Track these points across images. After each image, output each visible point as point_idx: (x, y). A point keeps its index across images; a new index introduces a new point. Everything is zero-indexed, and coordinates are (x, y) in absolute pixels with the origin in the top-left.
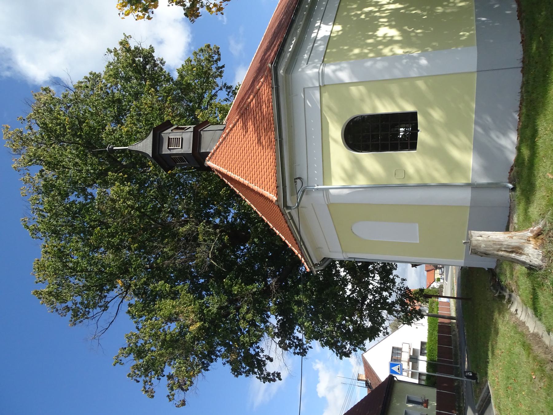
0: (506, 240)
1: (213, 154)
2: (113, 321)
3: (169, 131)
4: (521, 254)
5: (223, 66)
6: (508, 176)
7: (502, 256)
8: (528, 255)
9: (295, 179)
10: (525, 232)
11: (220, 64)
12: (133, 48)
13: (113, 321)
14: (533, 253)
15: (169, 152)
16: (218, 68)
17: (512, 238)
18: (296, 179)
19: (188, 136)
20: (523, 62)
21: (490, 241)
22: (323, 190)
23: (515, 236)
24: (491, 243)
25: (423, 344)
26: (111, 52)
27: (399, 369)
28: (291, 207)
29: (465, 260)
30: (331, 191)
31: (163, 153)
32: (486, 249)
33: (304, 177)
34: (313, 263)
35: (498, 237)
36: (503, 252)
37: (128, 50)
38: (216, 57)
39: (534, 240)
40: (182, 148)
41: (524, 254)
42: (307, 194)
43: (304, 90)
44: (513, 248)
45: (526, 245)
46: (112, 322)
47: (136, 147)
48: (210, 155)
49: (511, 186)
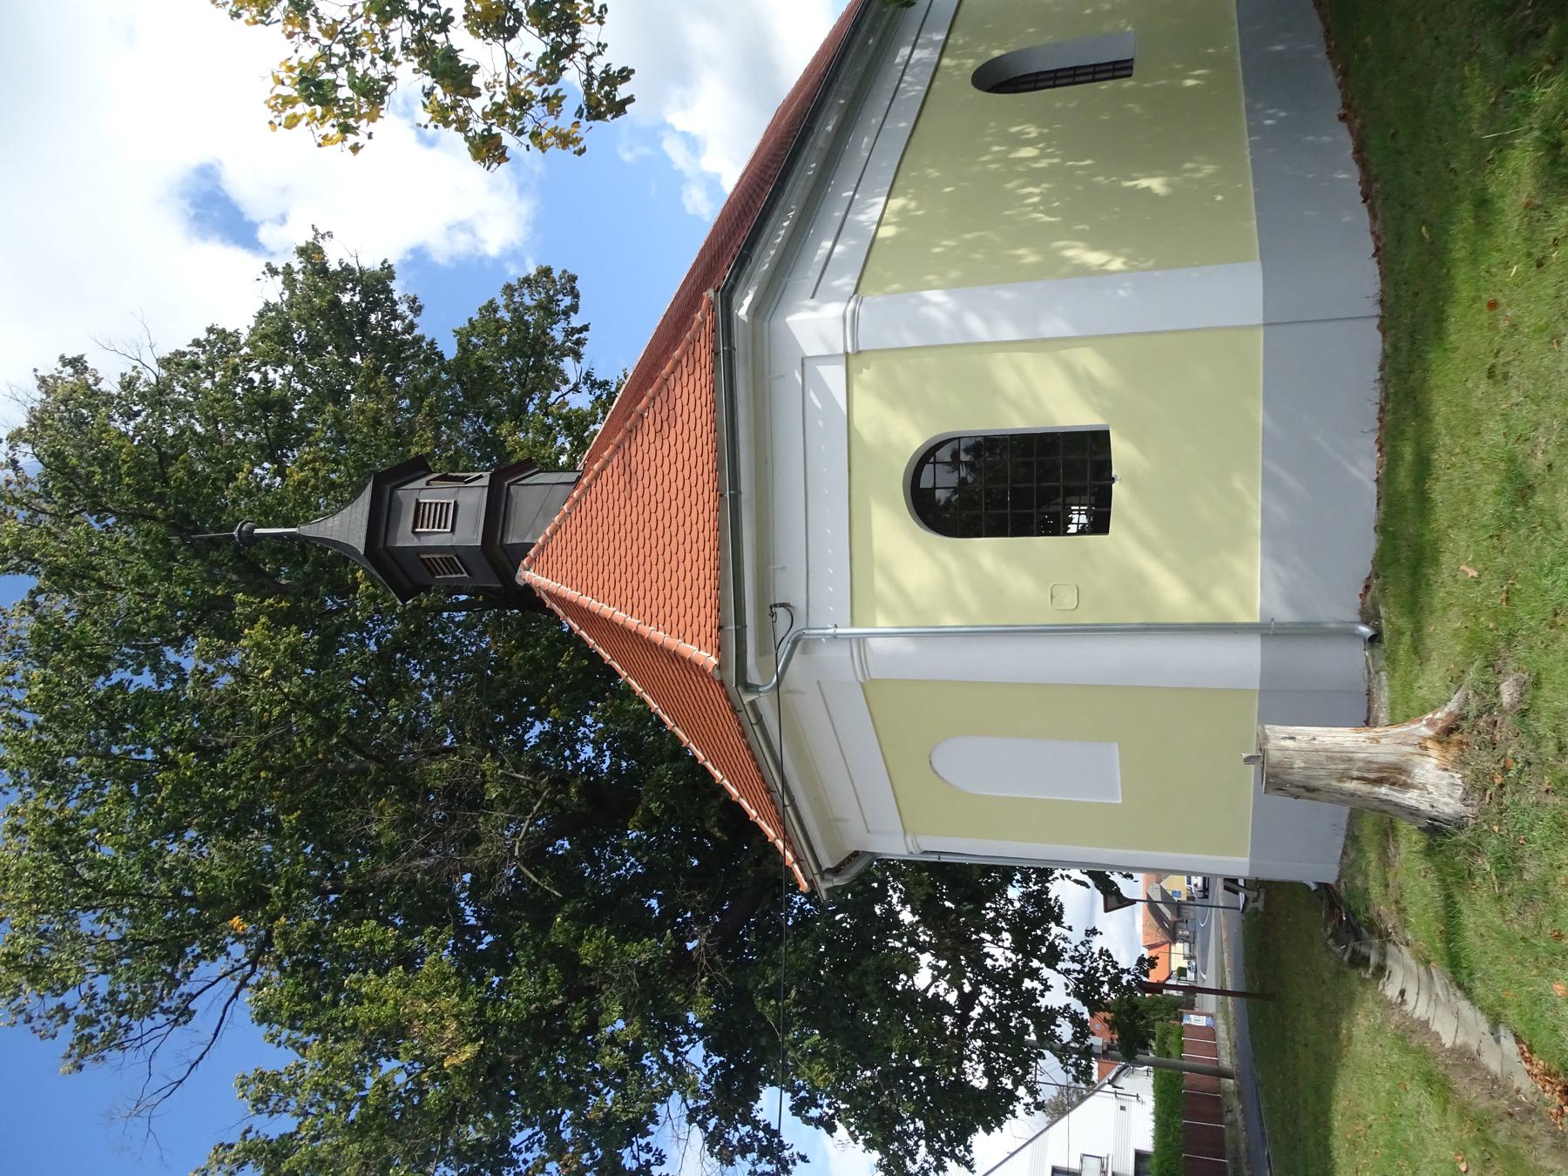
0: (1361, 748)
1: (542, 548)
2: (201, 1058)
3: (421, 483)
4: (1405, 786)
5: (585, 328)
6: (1359, 606)
7: (1352, 795)
8: (1423, 788)
9: (770, 609)
10: (1414, 726)
11: (576, 321)
12: (333, 266)
13: (201, 1058)
14: (1437, 780)
15: (414, 542)
16: (569, 333)
17: (1378, 742)
18: (775, 606)
19: (472, 498)
20: (1381, 302)
21: (1317, 751)
22: (849, 638)
23: (1386, 736)
24: (1321, 757)
25: (1140, 1156)
28: (758, 686)
29: (1252, 857)
30: (873, 642)
31: (399, 544)
32: (1309, 773)
33: (798, 601)
34: (818, 866)
35: (1338, 740)
36: (1355, 782)
37: (322, 270)
38: (567, 301)
39: (1439, 747)
40: (453, 530)
41: (1413, 786)
42: (804, 652)
43: (803, 365)
44: (1380, 770)
45: (1417, 759)
46: (197, 1062)
47: (322, 529)
48: (531, 553)
49: (1365, 630)
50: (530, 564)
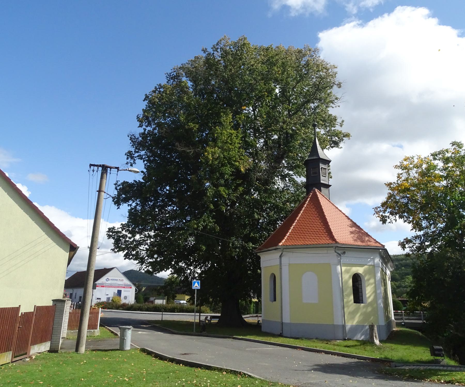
15: (320, 167)
26: (342, 122)
27: (196, 286)
31: (320, 164)
42: (337, 255)
50: (318, 192)
